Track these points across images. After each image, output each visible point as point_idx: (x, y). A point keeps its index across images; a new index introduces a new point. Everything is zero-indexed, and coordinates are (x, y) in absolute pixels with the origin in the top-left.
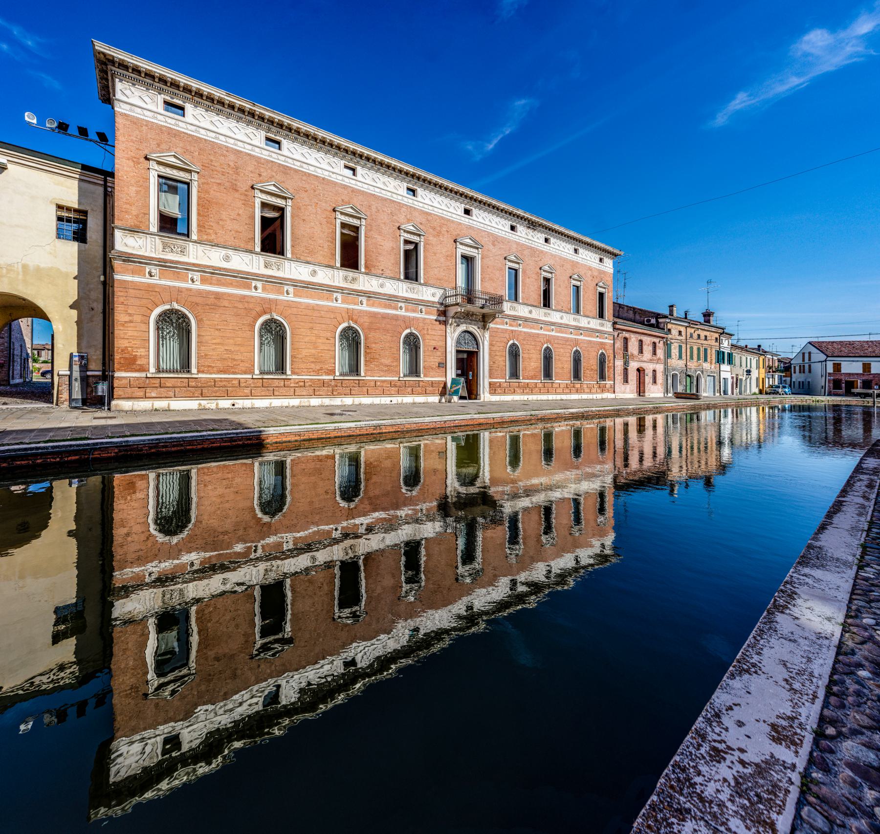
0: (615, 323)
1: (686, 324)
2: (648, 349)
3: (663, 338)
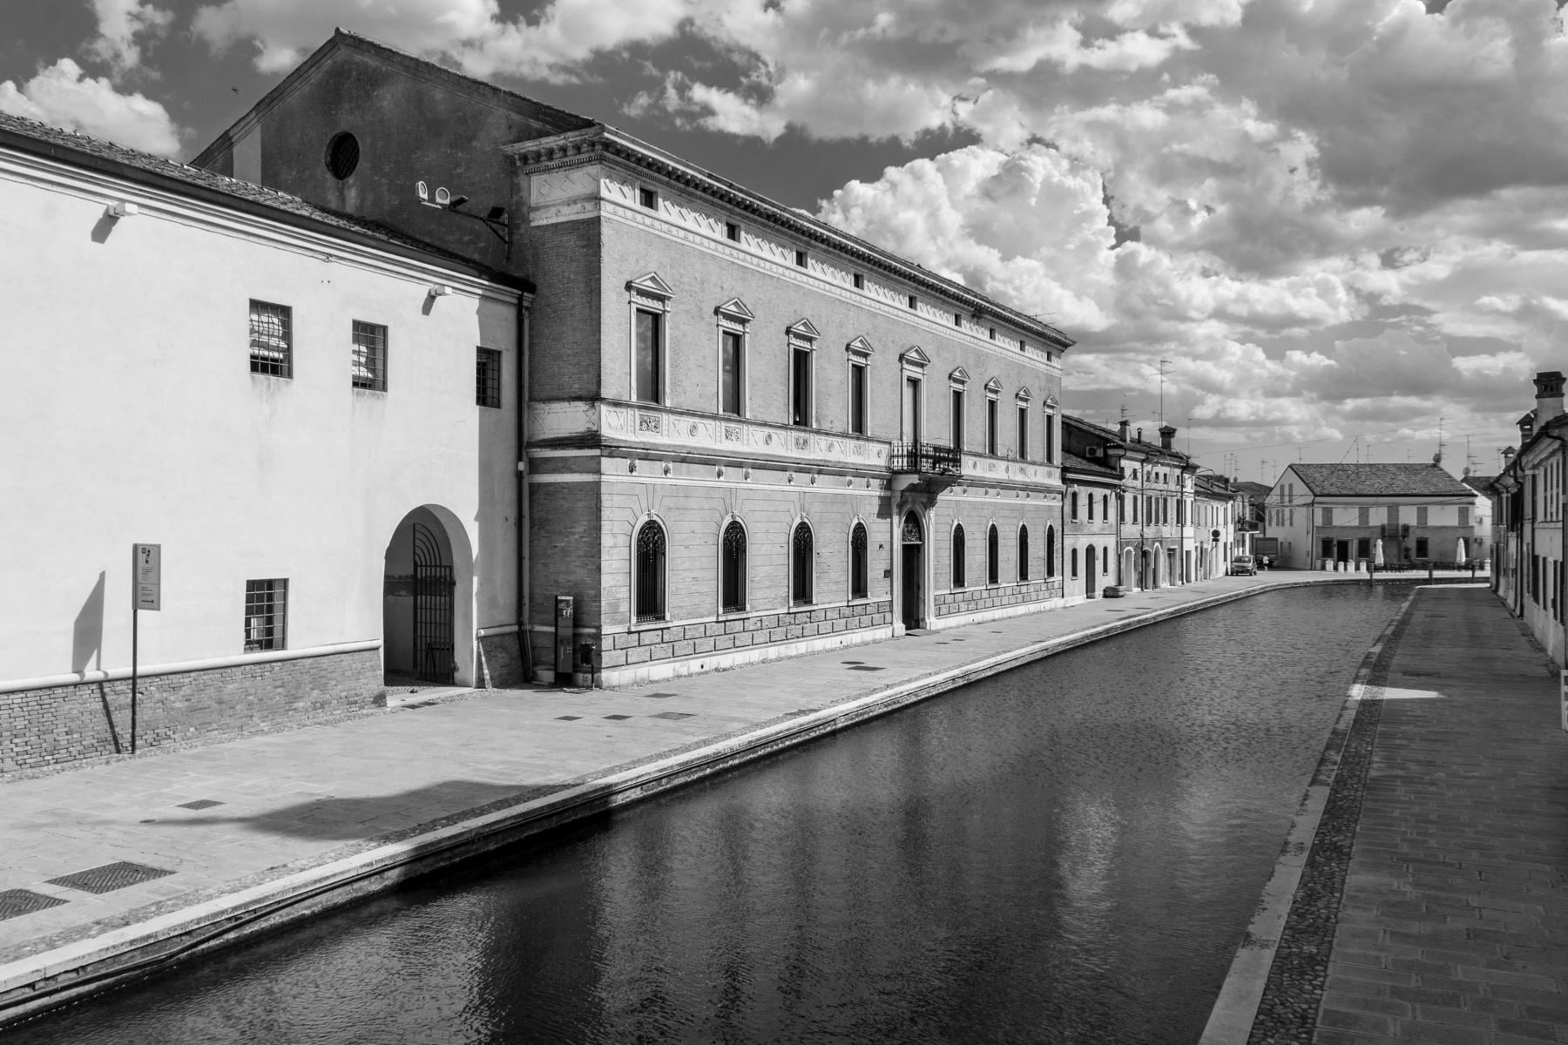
0: (1065, 470)
1: (1142, 457)
2: (1098, 509)
3: (1115, 486)
